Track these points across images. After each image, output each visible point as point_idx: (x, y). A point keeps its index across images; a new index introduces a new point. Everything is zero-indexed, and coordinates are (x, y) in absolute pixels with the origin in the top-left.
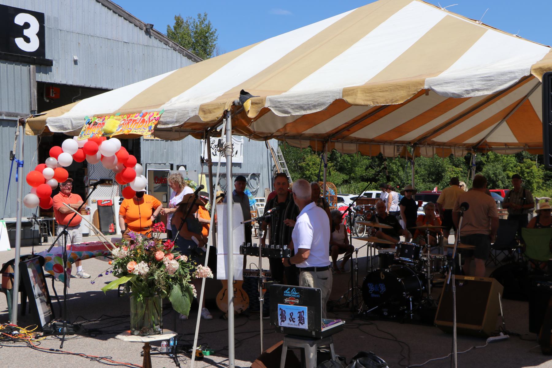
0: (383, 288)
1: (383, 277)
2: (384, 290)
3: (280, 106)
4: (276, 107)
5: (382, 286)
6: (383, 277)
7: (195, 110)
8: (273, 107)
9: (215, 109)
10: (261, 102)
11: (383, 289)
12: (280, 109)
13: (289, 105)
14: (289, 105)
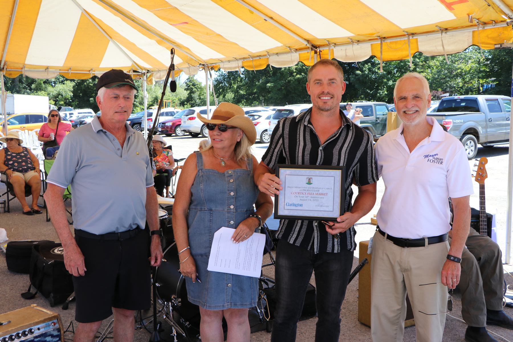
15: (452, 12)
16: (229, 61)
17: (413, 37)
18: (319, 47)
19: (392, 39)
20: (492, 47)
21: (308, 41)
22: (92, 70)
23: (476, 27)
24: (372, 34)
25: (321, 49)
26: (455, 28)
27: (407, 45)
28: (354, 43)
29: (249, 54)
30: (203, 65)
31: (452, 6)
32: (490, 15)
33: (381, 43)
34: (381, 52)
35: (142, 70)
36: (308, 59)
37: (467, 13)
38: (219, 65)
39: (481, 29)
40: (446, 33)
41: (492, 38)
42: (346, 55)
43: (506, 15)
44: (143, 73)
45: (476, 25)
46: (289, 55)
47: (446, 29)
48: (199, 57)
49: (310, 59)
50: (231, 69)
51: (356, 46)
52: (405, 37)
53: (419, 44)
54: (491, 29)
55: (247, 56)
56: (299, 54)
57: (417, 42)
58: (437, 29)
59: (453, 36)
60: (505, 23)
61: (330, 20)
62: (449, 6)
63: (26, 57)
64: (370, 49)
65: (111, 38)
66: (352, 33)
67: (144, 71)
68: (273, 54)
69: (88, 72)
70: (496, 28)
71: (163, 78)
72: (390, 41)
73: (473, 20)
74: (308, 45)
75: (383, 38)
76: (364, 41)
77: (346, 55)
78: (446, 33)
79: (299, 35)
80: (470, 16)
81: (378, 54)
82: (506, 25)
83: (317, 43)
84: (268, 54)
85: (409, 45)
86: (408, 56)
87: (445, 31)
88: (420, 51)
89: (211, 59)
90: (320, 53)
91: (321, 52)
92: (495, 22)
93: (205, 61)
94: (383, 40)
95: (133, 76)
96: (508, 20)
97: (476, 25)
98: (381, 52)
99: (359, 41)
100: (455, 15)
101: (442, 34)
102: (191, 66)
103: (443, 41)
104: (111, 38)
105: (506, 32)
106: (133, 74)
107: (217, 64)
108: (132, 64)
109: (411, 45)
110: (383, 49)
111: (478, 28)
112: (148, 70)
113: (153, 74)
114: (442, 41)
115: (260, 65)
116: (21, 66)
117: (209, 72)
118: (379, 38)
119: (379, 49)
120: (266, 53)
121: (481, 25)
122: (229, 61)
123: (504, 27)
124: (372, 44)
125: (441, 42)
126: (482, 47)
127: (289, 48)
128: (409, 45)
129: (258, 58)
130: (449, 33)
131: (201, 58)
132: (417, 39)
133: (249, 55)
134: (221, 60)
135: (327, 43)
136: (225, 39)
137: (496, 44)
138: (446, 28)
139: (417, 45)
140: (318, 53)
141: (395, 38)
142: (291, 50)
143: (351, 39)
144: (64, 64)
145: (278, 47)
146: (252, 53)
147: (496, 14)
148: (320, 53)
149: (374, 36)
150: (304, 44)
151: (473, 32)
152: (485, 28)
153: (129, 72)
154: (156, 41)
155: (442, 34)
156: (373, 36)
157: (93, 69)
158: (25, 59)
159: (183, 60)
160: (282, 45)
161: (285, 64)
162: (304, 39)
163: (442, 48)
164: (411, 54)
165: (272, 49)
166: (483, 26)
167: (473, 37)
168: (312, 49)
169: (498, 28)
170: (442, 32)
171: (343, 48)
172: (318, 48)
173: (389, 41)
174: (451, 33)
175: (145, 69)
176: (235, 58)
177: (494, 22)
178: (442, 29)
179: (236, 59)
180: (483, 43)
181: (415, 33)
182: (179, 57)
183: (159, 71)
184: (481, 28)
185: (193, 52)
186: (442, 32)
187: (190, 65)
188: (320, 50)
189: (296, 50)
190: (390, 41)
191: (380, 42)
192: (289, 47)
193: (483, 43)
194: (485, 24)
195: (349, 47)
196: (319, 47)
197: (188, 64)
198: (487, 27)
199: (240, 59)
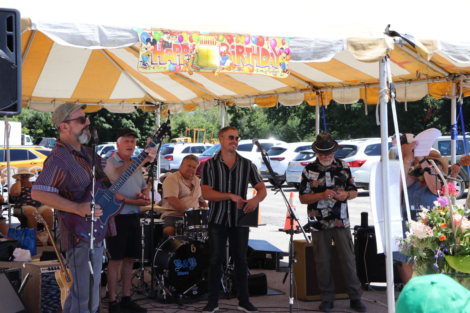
0: (193, 263)
1: (193, 249)
2: (194, 265)
3: (455, 51)
4: (450, 52)
5: (192, 261)
6: (193, 249)
7: (341, 42)
8: (446, 51)
9: (370, 45)
10: (431, 44)
11: (193, 264)
12: (455, 54)
13: (467, 52)
14: (467, 52)
15: (406, 70)
16: (243, 98)
18: (320, 89)
19: (373, 85)
20: (440, 97)
21: (309, 83)
22: (101, 101)
23: (427, 81)
24: (356, 81)
25: (322, 90)
29: (259, 93)
30: (218, 100)
31: (404, 65)
33: (366, 89)
34: (366, 97)
35: (156, 102)
36: (308, 100)
38: (234, 100)
40: (410, 83)
42: (342, 97)
44: (157, 105)
45: (424, 79)
46: (295, 94)
47: (411, 80)
48: (213, 93)
49: (310, 99)
50: (244, 106)
51: (347, 90)
55: (257, 94)
56: (305, 94)
59: (415, 86)
61: (317, 69)
62: (401, 65)
63: (33, 90)
64: (359, 93)
65: (123, 69)
66: (340, 79)
67: (158, 103)
68: (282, 93)
69: (97, 105)
70: (440, 82)
71: (179, 111)
72: (373, 87)
73: (421, 74)
74: (309, 87)
76: (354, 86)
77: (342, 97)
79: (300, 78)
80: (419, 72)
81: (364, 98)
82: (446, 81)
83: (319, 85)
84: (275, 94)
87: (409, 82)
89: (224, 95)
90: (321, 94)
91: (323, 93)
93: (219, 97)
94: (367, 86)
95: (146, 108)
98: (366, 97)
99: (350, 85)
100: (409, 71)
102: (205, 100)
104: (123, 69)
106: (146, 106)
107: (232, 100)
108: (145, 95)
110: (367, 94)
112: (162, 102)
113: (168, 106)
114: (406, 90)
115: (271, 103)
116: (27, 98)
117: (224, 107)
120: (274, 92)
121: (430, 79)
122: (243, 98)
124: (360, 89)
125: (404, 92)
127: (294, 89)
129: (269, 96)
130: (413, 84)
131: (214, 94)
133: (259, 94)
134: (234, 97)
135: (325, 85)
136: (233, 79)
137: (442, 95)
140: (320, 94)
141: (375, 85)
142: (295, 90)
143: (342, 84)
144: (72, 96)
145: (283, 88)
146: (261, 92)
148: (321, 94)
149: (358, 83)
150: (305, 86)
153: (142, 104)
154: (169, 76)
157: (103, 101)
158: (32, 92)
159: (197, 95)
160: (285, 86)
161: (292, 103)
162: (305, 81)
163: (404, 95)
165: (279, 89)
166: (432, 80)
167: (429, 88)
168: (313, 91)
171: (340, 90)
172: (319, 90)
173: (372, 87)
174: (413, 83)
175: (159, 101)
176: (247, 96)
177: (438, 78)
179: (248, 97)
180: (436, 94)
182: (193, 92)
183: (174, 104)
185: (207, 88)
186: (406, 83)
187: (205, 100)
188: (321, 92)
189: (302, 90)
190: (373, 87)
191: (364, 87)
192: (294, 88)
193: (436, 94)
194: (434, 78)
195: (342, 90)
196: (320, 89)
197: (203, 99)
199: (253, 96)
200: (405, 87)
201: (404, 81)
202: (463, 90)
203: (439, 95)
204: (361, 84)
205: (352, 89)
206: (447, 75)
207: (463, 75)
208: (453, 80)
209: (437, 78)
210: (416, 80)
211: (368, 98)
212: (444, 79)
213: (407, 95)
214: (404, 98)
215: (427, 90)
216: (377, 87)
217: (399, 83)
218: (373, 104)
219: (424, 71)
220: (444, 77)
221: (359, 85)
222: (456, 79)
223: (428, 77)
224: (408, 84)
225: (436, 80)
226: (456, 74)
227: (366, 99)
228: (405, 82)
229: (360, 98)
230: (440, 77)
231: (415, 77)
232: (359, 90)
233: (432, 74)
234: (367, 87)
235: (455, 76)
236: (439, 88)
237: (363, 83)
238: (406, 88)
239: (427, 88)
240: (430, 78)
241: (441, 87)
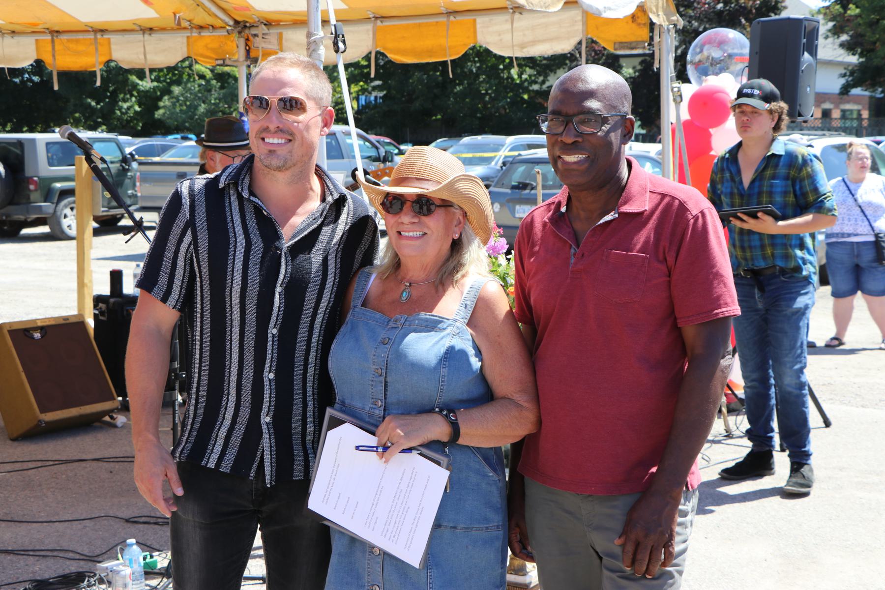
15: (153, 9)
17: (102, 35)
19: (70, 34)
24: (35, 25)
26: (163, 29)
27: (92, 49)
28: (6, 35)
32: (201, 18)
33: (53, 41)
34: (54, 56)
37: (173, 11)
39: (196, 34)
40: (150, 34)
41: (213, 50)
43: (223, 21)
45: (185, 28)
47: (151, 29)
52: (86, 34)
53: (113, 47)
54: (210, 36)
57: (109, 43)
58: (138, 28)
60: (224, 30)
64: (33, 47)
70: (214, 36)
73: (181, 20)
75: (55, 33)
78: (150, 34)
80: (178, 15)
81: (47, 59)
82: (226, 33)
85: (97, 49)
86: (94, 66)
87: (149, 32)
88: (113, 58)
92: (212, 26)
94: (55, 34)
96: (229, 28)
97: (185, 28)
98: (54, 56)
99: (13, 32)
100: (157, 12)
101: (144, 36)
103: (146, 47)
105: (229, 43)
109: (100, 48)
111: (191, 33)
118: (47, 31)
119: (50, 48)
121: (194, 30)
123: (225, 36)
124: (37, 40)
125: (142, 49)
126: (199, 60)
128: (97, 49)
130: (155, 36)
132: (109, 39)
137: (217, 59)
138: (151, 27)
139: (110, 48)
141: (74, 34)
147: (210, 17)
151: (188, 37)
152: (202, 34)
155: (144, 36)
156: (37, 27)
163: (142, 57)
164: (100, 63)
166: (198, 31)
167: (188, 45)
169: (219, 36)
170: (144, 34)
173: (65, 37)
177: (211, 28)
178: (143, 28)
180: (202, 56)
181: (106, 30)
184: (196, 33)
186: (144, 34)
193: (202, 56)
194: (201, 28)
198: (205, 33)
200: (144, 41)
201: (141, 30)
202: (262, 51)
203: (211, 58)
204: (44, 30)
205: (17, 39)
206: (231, 23)
207: (263, 26)
208: (240, 33)
209: (208, 28)
210: (172, 29)
211: (57, 57)
212: (222, 30)
213: (148, 57)
214: (143, 61)
215: (185, 49)
216: (77, 37)
217: (126, 33)
218: (66, 69)
219: (183, 14)
220: (221, 27)
221: (34, 32)
222: (247, 31)
223: (192, 25)
224: (147, 36)
225: (206, 30)
226: (247, 22)
227: (55, 59)
228: (141, 32)
229: (36, 58)
230: (212, 26)
231: (172, 24)
232: (34, 42)
233: (198, 21)
234: (55, 38)
235: (245, 27)
236: (210, 46)
237: (48, 29)
238: (146, 43)
239: (185, 44)
240: (195, 28)
241: (215, 45)
